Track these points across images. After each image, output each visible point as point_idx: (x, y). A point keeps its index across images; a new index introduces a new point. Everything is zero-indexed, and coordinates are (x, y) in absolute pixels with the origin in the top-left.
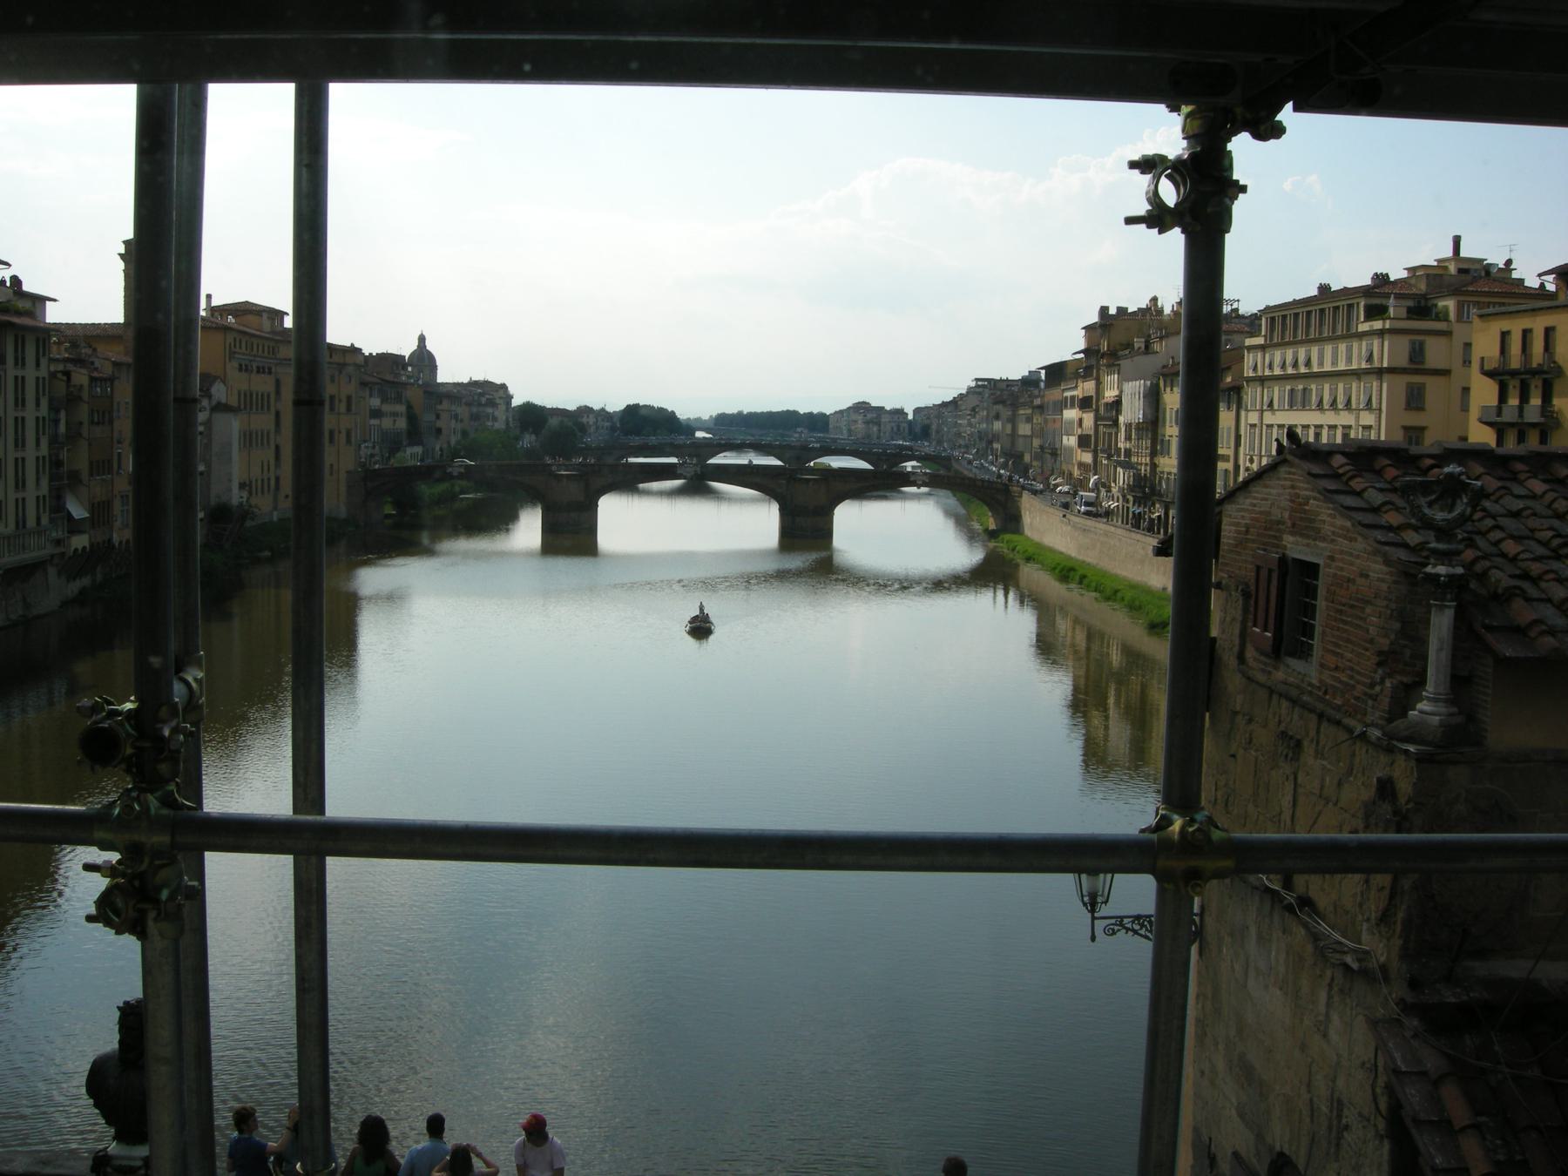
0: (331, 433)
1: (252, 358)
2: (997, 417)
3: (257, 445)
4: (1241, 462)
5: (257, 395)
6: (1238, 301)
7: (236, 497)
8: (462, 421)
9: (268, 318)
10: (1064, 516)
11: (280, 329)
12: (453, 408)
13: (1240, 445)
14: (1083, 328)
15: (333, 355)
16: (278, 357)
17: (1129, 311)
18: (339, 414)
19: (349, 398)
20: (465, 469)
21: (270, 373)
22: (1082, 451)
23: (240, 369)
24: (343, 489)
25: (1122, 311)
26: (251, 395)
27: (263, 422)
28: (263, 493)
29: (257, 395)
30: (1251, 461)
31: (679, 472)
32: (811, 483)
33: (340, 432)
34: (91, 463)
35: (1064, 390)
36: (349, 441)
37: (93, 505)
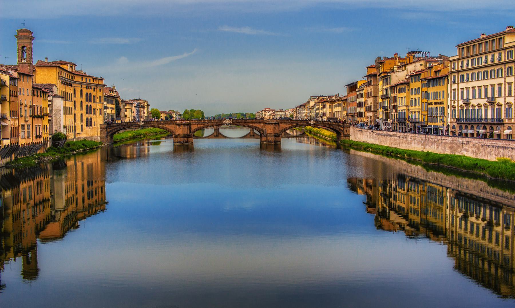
0: (94, 110)
2: (324, 107)
3: (68, 113)
4: (449, 103)
5: (68, 94)
6: (430, 52)
7: (63, 131)
9: (70, 66)
10: (372, 131)
11: (75, 71)
12: (131, 107)
13: (449, 98)
14: (366, 68)
15: (94, 80)
18: (97, 103)
21: (72, 86)
23: (62, 83)
25: (386, 58)
27: (70, 104)
28: (70, 131)
29: (68, 94)
30: (454, 103)
32: (273, 125)
33: (97, 110)
34: (10, 111)
35: (357, 92)
36: (100, 113)
37: (11, 128)
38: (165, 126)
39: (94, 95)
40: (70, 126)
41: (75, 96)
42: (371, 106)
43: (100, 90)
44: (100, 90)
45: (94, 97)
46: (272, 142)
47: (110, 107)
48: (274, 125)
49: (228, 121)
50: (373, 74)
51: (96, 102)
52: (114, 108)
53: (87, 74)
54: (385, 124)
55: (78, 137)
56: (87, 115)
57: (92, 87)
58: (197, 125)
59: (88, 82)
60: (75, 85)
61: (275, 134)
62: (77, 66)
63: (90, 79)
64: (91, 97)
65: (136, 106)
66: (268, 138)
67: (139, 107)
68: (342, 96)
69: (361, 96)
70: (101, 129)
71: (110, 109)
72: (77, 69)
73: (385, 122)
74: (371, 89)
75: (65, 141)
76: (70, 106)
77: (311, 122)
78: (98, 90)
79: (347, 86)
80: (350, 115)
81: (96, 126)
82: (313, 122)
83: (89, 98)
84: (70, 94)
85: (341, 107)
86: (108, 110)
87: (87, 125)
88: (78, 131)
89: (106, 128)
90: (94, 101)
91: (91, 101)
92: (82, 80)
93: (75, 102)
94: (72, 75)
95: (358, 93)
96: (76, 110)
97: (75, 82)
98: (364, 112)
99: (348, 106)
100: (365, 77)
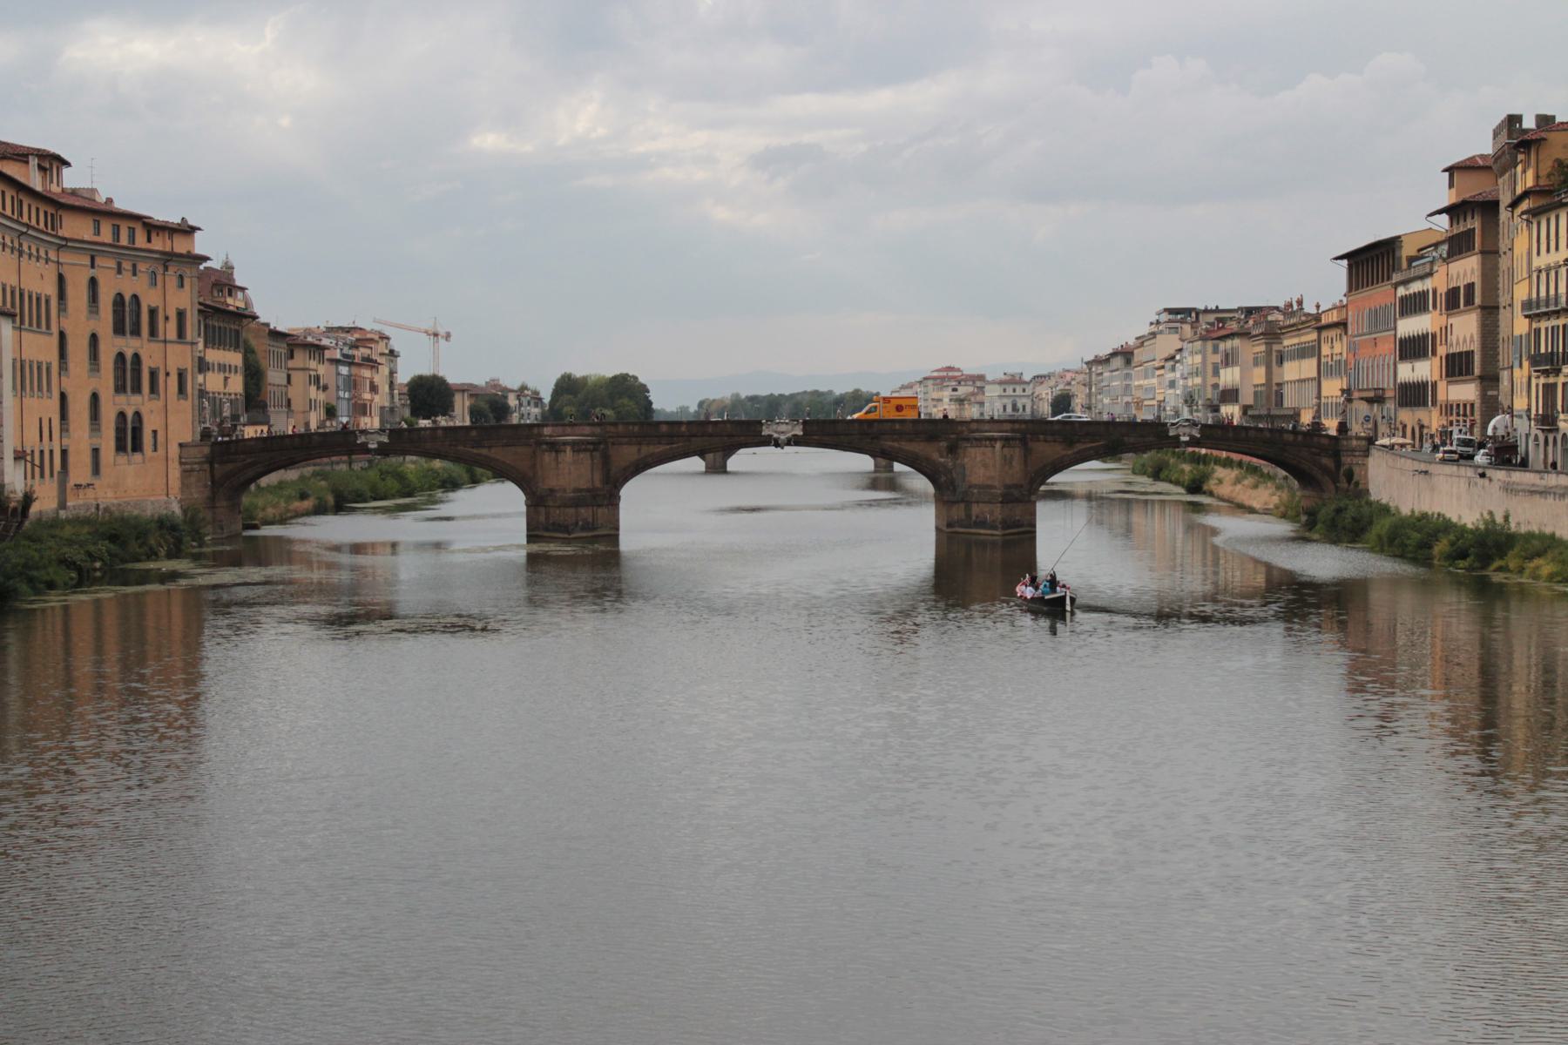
0: (153, 374)
1: (25, 230)
2: (1229, 360)
3: (32, 389)
5: (30, 297)
8: (325, 388)
9: (41, 168)
11: (59, 190)
12: (313, 364)
14: (1445, 170)
16: (60, 234)
17: (1558, 120)
18: (165, 341)
19: (181, 315)
20: (390, 437)
22: (1449, 383)
24: (175, 472)
25: (1545, 121)
26: (22, 295)
27: (41, 348)
28: (42, 475)
29: (30, 297)
31: (765, 432)
32: (998, 445)
35: (1396, 286)
38: (484, 451)
39: (153, 305)
40: (42, 452)
41: (65, 310)
42: (1470, 354)
43: (181, 277)
44: (181, 277)
45: (153, 312)
46: (994, 527)
47: (219, 365)
48: (1003, 447)
49: (783, 428)
50: (1481, 199)
51: (161, 337)
52: (236, 367)
53: (120, 205)
54: (1541, 437)
55: (81, 502)
56: (122, 398)
57: (142, 267)
58: (640, 444)
59: (124, 241)
60: (66, 258)
61: (1008, 487)
62: (67, 164)
63: (134, 229)
64: (138, 315)
65: (338, 356)
66: (975, 509)
67: (350, 364)
68: (1318, 307)
69: (1414, 305)
70: (185, 464)
71: (219, 370)
72: (71, 179)
73: (1543, 430)
74: (1467, 269)
75: (21, 523)
76: (41, 358)
77: (1181, 431)
78: (172, 281)
79: (1345, 262)
80: (1362, 399)
81: (161, 451)
82: (1187, 430)
83: (127, 316)
84: (38, 299)
85: (1314, 361)
86: (209, 375)
87: (120, 447)
88: (80, 471)
89: (210, 461)
90: (153, 332)
91: (136, 332)
92: (98, 233)
93: (62, 335)
94: (51, 210)
95: (1401, 291)
96: (68, 377)
97: (65, 244)
98: (1434, 385)
99: (1351, 356)
100: (1440, 212)
